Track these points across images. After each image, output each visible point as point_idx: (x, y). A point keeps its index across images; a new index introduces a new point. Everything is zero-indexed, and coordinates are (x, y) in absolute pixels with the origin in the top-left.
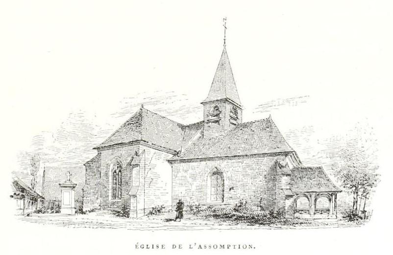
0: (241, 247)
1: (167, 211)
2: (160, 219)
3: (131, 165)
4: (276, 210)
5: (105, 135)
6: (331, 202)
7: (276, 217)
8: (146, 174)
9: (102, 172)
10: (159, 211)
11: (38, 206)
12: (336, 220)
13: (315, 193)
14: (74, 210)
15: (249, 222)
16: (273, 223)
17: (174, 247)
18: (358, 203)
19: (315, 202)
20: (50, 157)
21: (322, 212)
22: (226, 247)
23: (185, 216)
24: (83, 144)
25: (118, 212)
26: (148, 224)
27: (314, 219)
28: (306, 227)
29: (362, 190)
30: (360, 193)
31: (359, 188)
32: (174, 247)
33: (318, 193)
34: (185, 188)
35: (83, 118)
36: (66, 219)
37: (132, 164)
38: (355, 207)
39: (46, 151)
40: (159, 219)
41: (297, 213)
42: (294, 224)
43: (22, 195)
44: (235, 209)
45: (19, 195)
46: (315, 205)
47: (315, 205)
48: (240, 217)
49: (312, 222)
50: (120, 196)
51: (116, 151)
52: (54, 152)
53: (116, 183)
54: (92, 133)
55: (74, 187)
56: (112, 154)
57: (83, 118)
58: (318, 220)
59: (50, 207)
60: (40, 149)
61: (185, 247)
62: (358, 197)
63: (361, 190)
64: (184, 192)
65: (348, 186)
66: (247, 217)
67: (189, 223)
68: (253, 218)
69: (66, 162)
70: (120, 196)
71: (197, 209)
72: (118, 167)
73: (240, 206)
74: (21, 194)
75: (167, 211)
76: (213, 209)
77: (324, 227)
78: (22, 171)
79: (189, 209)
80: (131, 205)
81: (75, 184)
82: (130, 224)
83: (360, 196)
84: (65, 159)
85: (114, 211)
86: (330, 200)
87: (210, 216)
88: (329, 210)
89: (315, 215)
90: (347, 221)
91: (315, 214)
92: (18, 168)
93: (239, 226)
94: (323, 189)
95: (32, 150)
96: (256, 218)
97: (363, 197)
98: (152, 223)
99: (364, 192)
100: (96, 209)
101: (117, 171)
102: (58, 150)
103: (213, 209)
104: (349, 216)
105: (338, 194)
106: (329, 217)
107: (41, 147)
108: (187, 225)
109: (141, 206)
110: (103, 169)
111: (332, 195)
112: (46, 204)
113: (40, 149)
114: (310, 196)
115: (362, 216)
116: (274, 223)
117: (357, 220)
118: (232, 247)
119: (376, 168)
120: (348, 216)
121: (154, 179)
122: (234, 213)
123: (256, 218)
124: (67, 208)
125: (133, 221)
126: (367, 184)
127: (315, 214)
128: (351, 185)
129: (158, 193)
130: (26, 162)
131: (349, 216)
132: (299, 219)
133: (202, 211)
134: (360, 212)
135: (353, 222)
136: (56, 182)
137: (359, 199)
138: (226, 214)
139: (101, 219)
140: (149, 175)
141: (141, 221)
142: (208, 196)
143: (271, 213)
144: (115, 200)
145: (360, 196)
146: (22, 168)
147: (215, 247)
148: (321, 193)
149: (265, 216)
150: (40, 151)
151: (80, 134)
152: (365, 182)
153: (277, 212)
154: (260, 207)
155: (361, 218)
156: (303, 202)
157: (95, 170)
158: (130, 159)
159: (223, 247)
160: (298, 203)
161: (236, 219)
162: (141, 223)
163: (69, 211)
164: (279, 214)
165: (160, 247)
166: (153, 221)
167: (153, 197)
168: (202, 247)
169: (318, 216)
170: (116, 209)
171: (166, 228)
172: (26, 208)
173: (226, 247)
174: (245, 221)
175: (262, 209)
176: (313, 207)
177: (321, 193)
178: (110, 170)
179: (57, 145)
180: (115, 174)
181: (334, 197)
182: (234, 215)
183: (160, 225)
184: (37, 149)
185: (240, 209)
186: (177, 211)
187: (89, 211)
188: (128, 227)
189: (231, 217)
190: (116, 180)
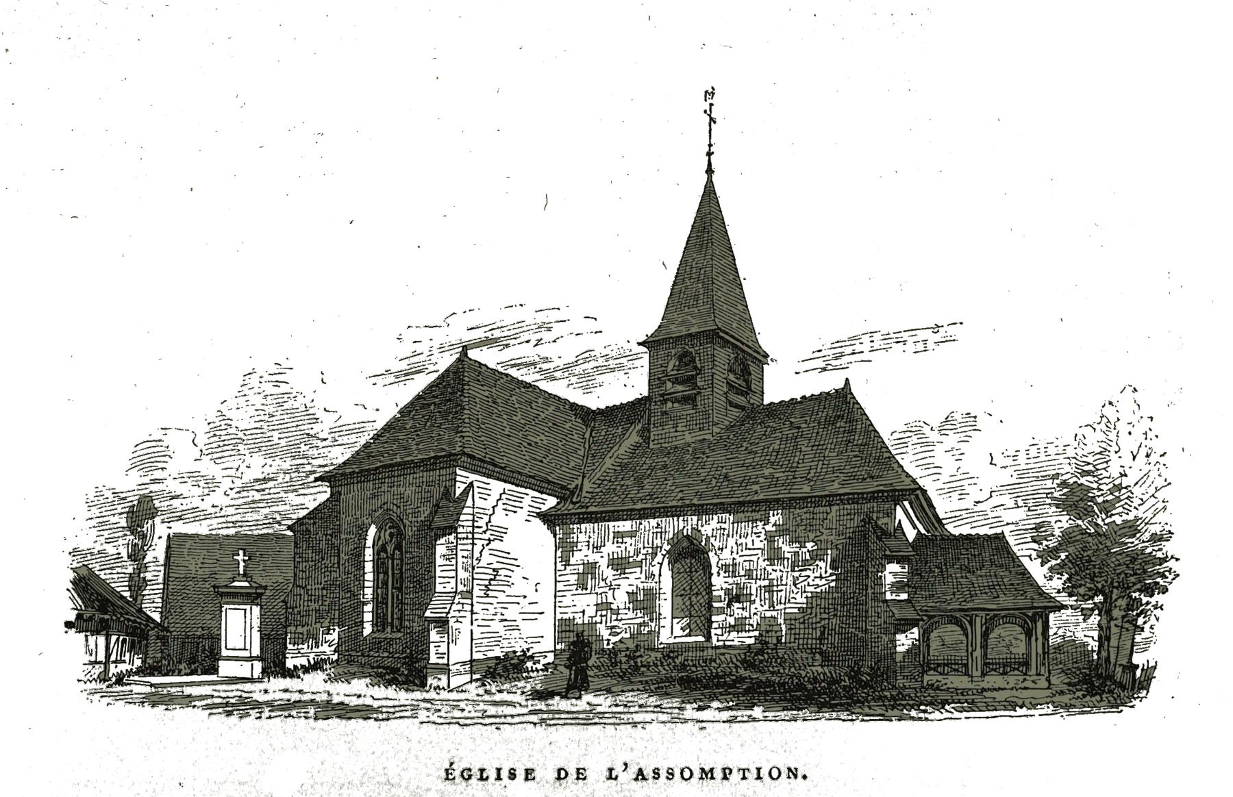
0: (764, 773)
1: (540, 667)
2: (519, 692)
3: (430, 528)
4: (869, 662)
5: (353, 438)
6: (1033, 639)
7: (867, 685)
8: (477, 555)
9: (344, 548)
10: (515, 666)
11: (150, 654)
12: (1048, 692)
13: (983, 614)
14: (258, 666)
15: (789, 701)
16: (859, 701)
17: (563, 774)
18: (1114, 643)
19: (986, 641)
20: (188, 504)
21: (1005, 667)
22: (718, 774)
23: (594, 682)
24: (286, 466)
25: (395, 671)
26: (482, 707)
27: (984, 690)
28: (957, 715)
29: (1122, 603)
30: (1116, 613)
31: (1114, 597)
32: (563, 774)
33: (992, 613)
34: (592, 599)
35: (284, 388)
36: (234, 691)
37: (434, 525)
38: (1104, 654)
39: (173, 486)
40: (515, 694)
41: (931, 672)
42: (922, 704)
43: (102, 620)
44: (744, 661)
45: (91, 618)
46: (985, 646)
47: (985, 646)
48: (760, 684)
49: (977, 698)
50: (396, 622)
51: (385, 488)
52: (198, 491)
53: (387, 584)
54: (312, 432)
55: (260, 595)
56: (374, 496)
57: (284, 388)
58: (995, 694)
59: (187, 655)
60: (155, 481)
61: (596, 773)
62: (1113, 623)
63: (1119, 602)
64: (591, 611)
65: (1082, 590)
66: (781, 685)
67: (604, 703)
68: (801, 687)
69: (234, 519)
70: (396, 622)
71: (632, 662)
72: (391, 535)
73: (761, 652)
74: (98, 616)
75: (540, 667)
76: (678, 661)
77: (1012, 713)
78: (101, 548)
79: (605, 660)
80: (433, 650)
81: (261, 587)
82: (429, 705)
83: (1119, 622)
84: (231, 511)
85: (378, 667)
86: (1029, 633)
87: (670, 680)
88: (1026, 664)
89: (987, 678)
90: (1079, 694)
91: (983, 674)
92: (88, 540)
93: (757, 712)
94: (1006, 601)
95: (130, 483)
96: (810, 687)
97: (1126, 625)
98: (495, 703)
99: (1129, 608)
100: (324, 661)
101: (390, 548)
102: (211, 484)
103: (678, 661)
104: (1086, 680)
105: (1052, 617)
106: (1026, 684)
107: (158, 474)
108: (599, 709)
109: (460, 653)
110: (347, 540)
111: (1034, 622)
112: (175, 646)
113: (155, 481)
114: (970, 623)
115: (1126, 679)
116: (863, 703)
117: (1111, 692)
118: (736, 776)
119: (1157, 539)
120: (1084, 682)
121: (501, 572)
122: (742, 672)
123: (810, 687)
124: (237, 659)
125: (437, 697)
126: (1138, 586)
127: (983, 674)
128: (1090, 589)
129: (512, 613)
130: (113, 519)
131: (1086, 680)
132: (938, 688)
133: (648, 666)
134: (1119, 670)
135: (1098, 698)
136: (204, 580)
137: (1114, 630)
138: (717, 676)
139: (341, 691)
140: (486, 559)
141: (462, 696)
142: (663, 622)
143: (855, 675)
144: (383, 636)
145: (1119, 622)
146: (102, 540)
147: (686, 775)
148: (1003, 613)
149: (838, 682)
150: (154, 487)
151: (276, 435)
152: (1132, 579)
153: (872, 668)
154: (821, 654)
155: (1123, 687)
156: (948, 640)
157: (323, 545)
158: (426, 511)
159: (707, 774)
160: (935, 644)
161: (747, 691)
162: (462, 705)
163: (243, 670)
164: (874, 672)
165: (521, 774)
166: (498, 697)
167: (497, 626)
168: (648, 772)
169: (993, 680)
170: (388, 662)
171: (534, 718)
172: (113, 658)
173: (718, 774)
174: (777, 697)
175: (826, 659)
176: (978, 653)
177: (1003, 613)
178: (369, 543)
179: (207, 467)
180: (383, 555)
181: (1039, 624)
182: (742, 679)
183: (519, 710)
184: (147, 480)
185: (761, 662)
186: (569, 667)
187: (303, 666)
188: (423, 715)
189: (733, 685)
190: (386, 573)
